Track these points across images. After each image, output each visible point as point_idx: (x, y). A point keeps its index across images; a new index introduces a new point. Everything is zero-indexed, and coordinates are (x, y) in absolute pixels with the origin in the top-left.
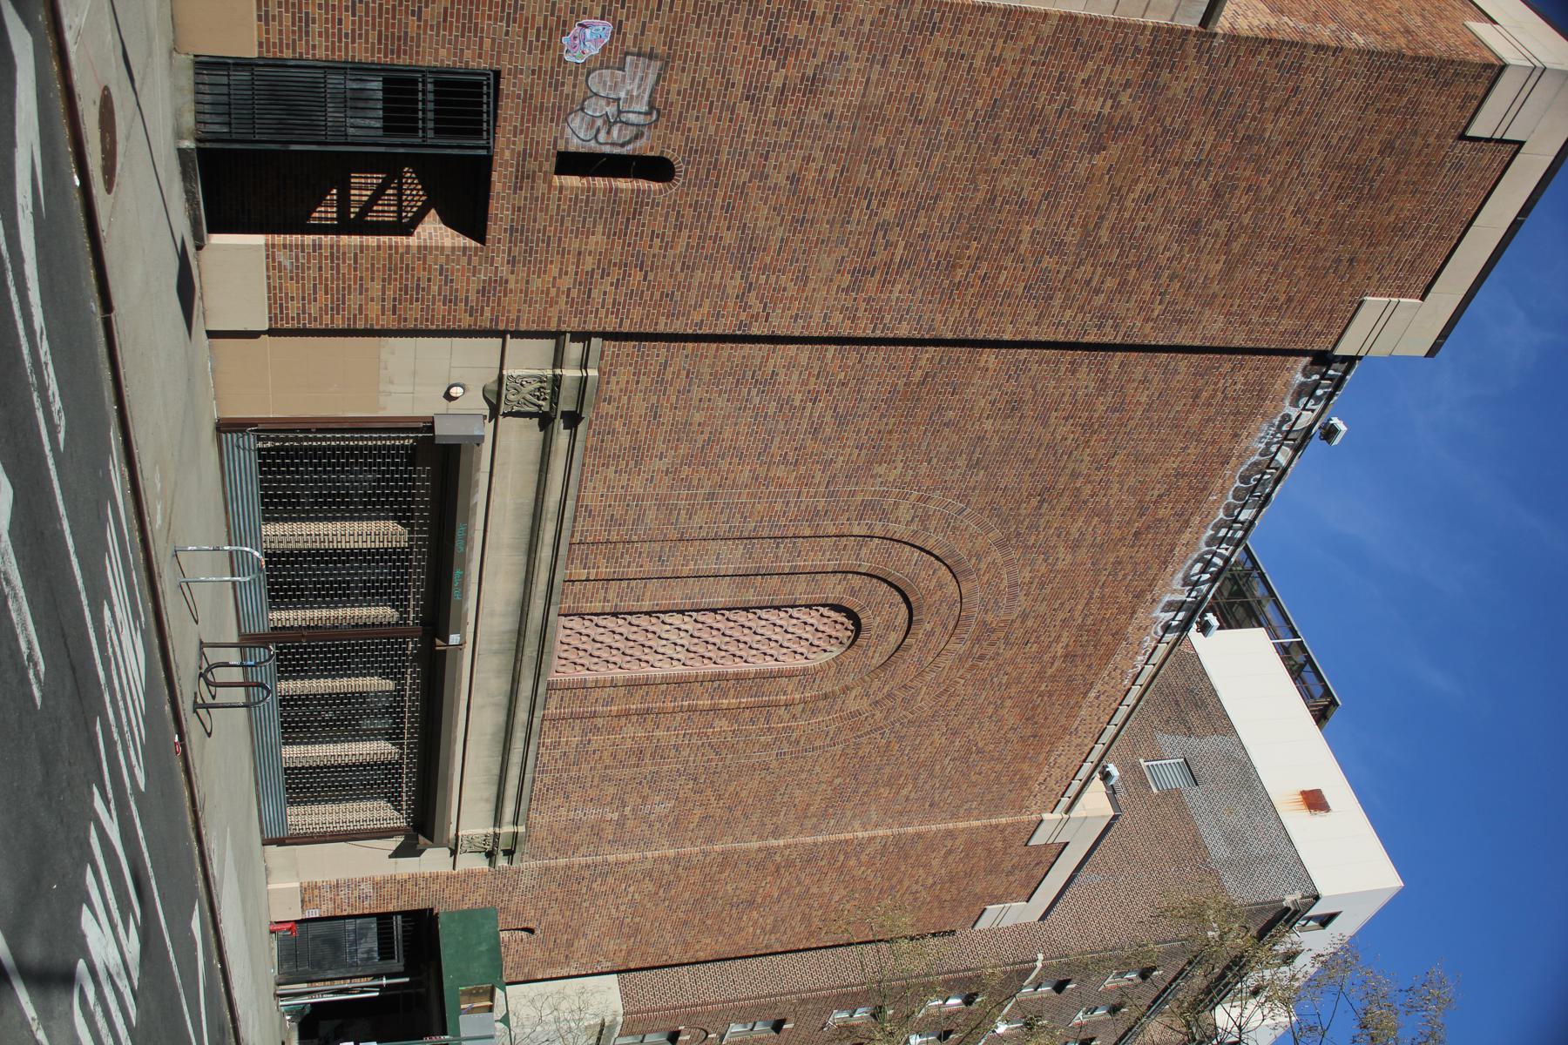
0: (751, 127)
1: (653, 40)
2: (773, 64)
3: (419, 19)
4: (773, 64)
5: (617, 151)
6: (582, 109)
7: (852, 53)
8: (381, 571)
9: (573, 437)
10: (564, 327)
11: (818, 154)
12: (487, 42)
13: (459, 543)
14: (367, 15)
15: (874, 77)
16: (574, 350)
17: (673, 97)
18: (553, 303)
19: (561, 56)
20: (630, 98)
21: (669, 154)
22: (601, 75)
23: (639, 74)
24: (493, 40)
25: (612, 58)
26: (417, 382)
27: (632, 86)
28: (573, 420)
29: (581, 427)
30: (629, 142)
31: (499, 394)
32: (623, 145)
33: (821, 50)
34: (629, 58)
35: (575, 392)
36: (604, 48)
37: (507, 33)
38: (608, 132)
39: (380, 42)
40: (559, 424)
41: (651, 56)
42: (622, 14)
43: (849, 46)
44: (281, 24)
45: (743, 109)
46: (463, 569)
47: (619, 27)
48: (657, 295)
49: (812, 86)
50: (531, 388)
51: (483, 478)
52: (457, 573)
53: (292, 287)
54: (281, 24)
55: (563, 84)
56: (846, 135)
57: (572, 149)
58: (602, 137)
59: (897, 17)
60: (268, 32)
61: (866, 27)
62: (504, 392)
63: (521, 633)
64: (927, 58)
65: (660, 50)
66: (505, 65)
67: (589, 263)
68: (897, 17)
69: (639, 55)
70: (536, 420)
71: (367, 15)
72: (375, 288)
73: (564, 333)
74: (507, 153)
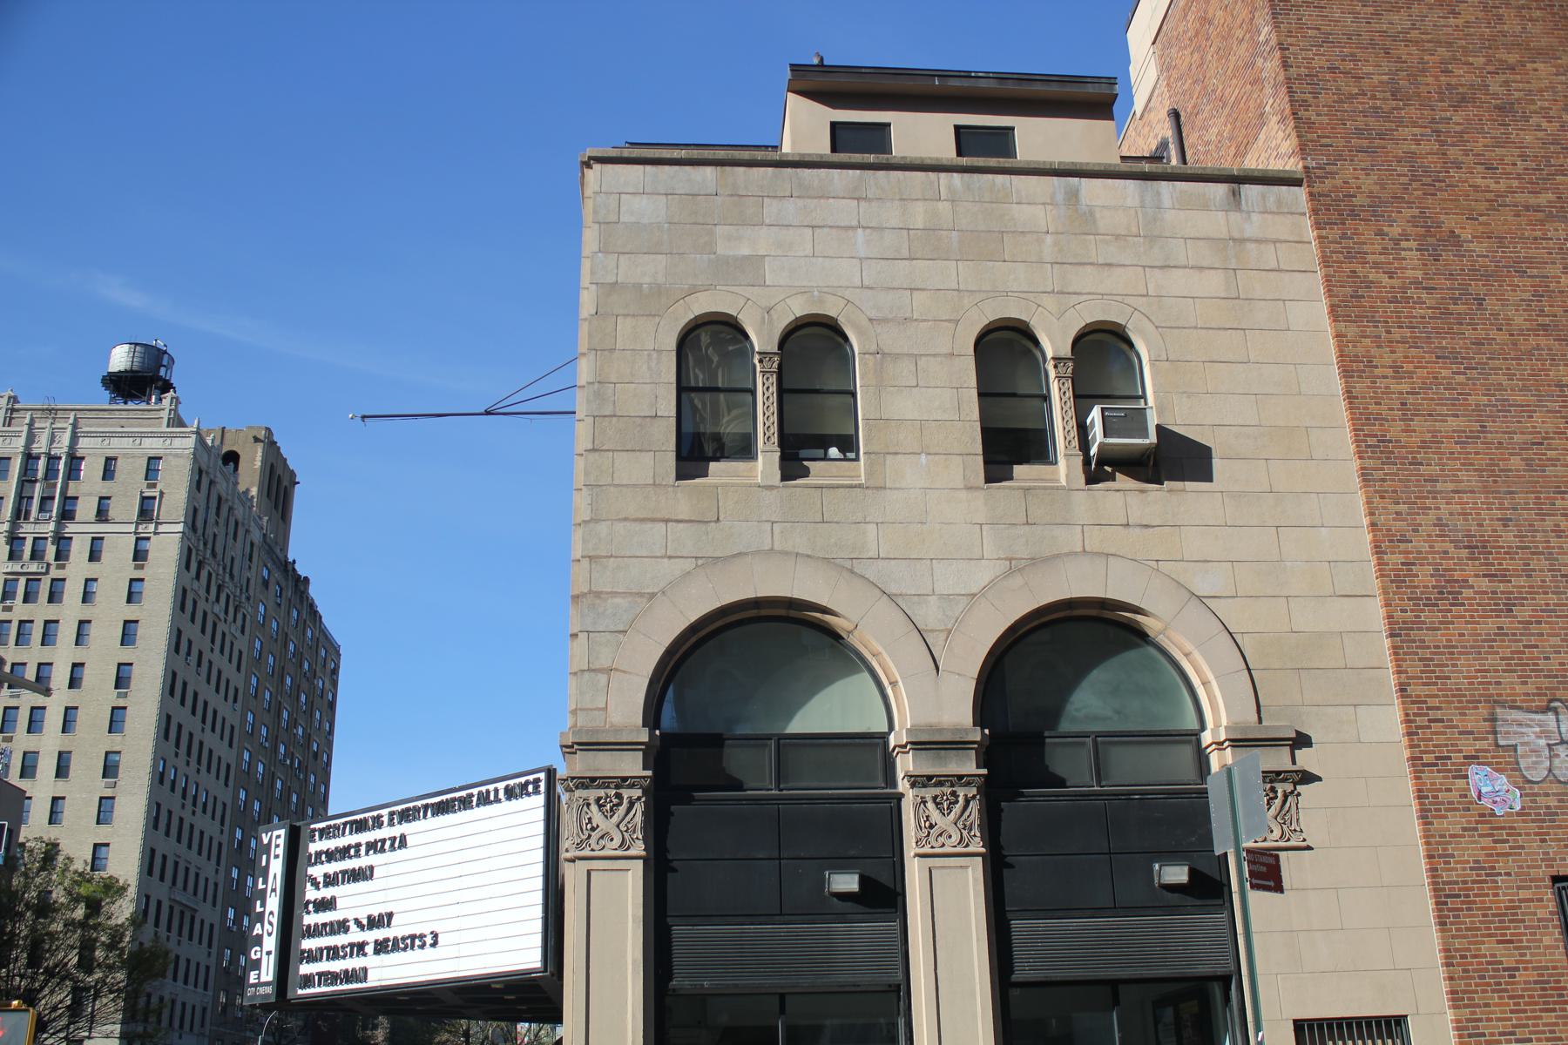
0: (1540, 600)
1: (1475, 719)
2: (1467, 593)
3: (1517, 969)
7: (1432, 515)
11: (1549, 523)
12: (1523, 894)
14: (1526, 1026)
15: (1450, 486)
17: (1531, 688)
19: (1518, 814)
20: (1545, 733)
22: (1528, 769)
23: (1515, 728)
24: (1519, 888)
25: (1505, 760)
27: (1531, 734)
33: (1438, 547)
34: (1501, 742)
36: (1496, 770)
37: (1508, 874)
39: (1554, 1010)
42: (1457, 758)
43: (1426, 521)
45: (1523, 613)
47: (1472, 758)
49: (1477, 548)
55: (1548, 807)
56: (1520, 499)
59: (1384, 480)
61: (1403, 508)
64: (1415, 439)
65: (1483, 711)
66: (1544, 872)
68: (1384, 480)
71: (1526, 1026)
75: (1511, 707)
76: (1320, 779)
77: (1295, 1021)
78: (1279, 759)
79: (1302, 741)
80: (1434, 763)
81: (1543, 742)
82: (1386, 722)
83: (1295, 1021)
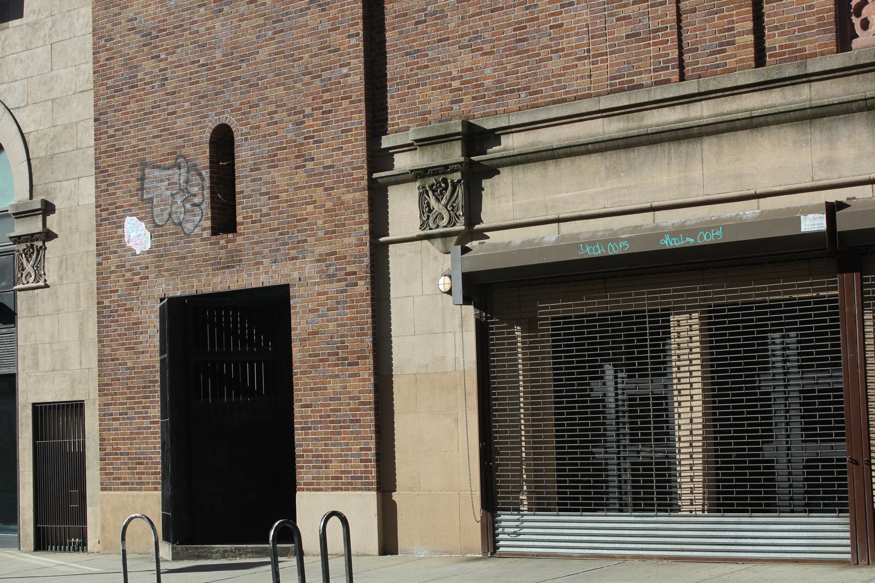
4: (140, 75)
5: (207, 183)
6: (180, 224)
8: (782, 346)
9: (508, 130)
10: (364, 183)
13: (614, 250)
16: (403, 162)
17: (166, 150)
18: (340, 203)
19: (148, 252)
21: (207, 136)
26: (435, 332)
28: (476, 138)
29: (489, 124)
30: (200, 175)
31: (444, 235)
32: (203, 179)
34: (145, 197)
35: (438, 147)
38: (195, 195)
40: (494, 152)
41: (142, 179)
44: (143, 473)
46: (662, 235)
48: (326, 96)
50: (433, 202)
51: (748, 210)
52: (668, 243)
53: (335, 467)
54: (143, 473)
57: (208, 224)
58: (197, 200)
60: (148, 483)
67: (300, 177)
69: (142, 189)
70: (486, 183)
72: (334, 386)
73: (371, 181)
74: (218, 279)
75: (154, 167)
76: (56, 236)
77: (34, 405)
78: (34, 226)
79: (48, 208)
80: (108, 218)
81: (169, 193)
82: (87, 189)
83: (34, 405)
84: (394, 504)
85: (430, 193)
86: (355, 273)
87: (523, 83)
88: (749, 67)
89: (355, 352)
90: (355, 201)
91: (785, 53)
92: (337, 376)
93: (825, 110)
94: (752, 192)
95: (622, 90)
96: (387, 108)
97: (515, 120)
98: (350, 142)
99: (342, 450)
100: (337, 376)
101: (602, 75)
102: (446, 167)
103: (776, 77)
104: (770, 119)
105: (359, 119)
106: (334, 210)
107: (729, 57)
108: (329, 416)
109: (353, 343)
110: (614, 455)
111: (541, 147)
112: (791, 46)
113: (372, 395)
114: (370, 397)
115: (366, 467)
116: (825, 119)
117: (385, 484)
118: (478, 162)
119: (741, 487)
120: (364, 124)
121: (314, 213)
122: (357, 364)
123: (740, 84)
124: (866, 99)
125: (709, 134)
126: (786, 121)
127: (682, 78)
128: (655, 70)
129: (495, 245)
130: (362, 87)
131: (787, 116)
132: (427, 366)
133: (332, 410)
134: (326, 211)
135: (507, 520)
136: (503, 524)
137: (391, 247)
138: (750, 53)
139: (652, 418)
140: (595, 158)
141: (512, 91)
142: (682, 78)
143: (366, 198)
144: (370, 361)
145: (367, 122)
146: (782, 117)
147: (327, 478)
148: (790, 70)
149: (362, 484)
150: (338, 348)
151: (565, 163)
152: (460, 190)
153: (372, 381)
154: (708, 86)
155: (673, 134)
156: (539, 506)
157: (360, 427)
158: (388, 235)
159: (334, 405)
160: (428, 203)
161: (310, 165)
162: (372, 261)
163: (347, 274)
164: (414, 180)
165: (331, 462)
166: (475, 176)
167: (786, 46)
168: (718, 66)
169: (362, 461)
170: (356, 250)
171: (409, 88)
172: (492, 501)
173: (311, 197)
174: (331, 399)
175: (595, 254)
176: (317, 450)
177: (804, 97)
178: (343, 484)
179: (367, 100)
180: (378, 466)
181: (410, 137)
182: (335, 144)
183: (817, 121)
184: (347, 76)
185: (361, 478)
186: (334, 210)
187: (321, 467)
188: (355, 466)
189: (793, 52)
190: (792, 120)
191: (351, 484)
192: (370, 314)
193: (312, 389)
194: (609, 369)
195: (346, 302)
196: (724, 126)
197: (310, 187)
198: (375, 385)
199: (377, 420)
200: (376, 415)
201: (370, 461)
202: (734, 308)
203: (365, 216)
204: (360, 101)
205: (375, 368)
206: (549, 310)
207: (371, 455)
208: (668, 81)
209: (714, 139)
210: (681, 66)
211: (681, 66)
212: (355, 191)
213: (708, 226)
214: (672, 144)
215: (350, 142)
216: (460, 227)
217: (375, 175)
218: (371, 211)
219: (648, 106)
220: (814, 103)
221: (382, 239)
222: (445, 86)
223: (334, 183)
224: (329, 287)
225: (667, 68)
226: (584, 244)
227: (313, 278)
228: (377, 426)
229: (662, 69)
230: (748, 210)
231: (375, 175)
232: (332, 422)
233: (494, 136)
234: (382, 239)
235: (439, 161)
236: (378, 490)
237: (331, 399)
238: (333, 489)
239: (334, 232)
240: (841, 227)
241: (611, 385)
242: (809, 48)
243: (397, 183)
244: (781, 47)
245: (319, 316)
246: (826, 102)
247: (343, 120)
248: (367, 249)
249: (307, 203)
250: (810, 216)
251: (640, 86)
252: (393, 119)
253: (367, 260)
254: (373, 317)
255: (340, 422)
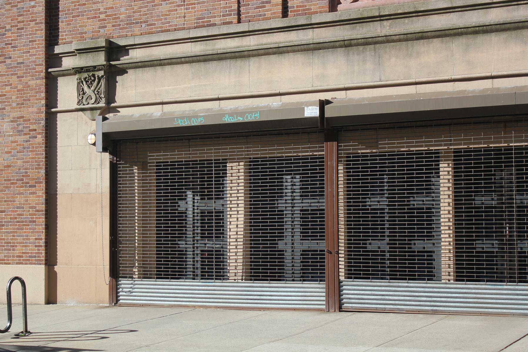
8: (291, 184)
9: (134, 46)
10: (43, 74)
13: (195, 122)
16: (68, 63)
28: (114, 51)
29: (122, 42)
31: (92, 109)
35: (90, 55)
40: (124, 60)
46: (224, 115)
48: (20, 19)
51: (275, 102)
52: (228, 120)
53: (19, 250)
62: (90, 106)
63: (347, 45)
70: (119, 78)
72: (20, 200)
84: (55, 273)
85: (84, 83)
86: (35, 130)
87: (144, 18)
88: (278, 17)
89: (33, 179)
90: (36, 85)
91: (299, 11)
92: (22, 194)
93: (321, 45)
94: (277, 92)
95: (204, 26)
96: (58, 29)
97: (138, 41)
98: (35, 48)
99: (24, 239)
100: (22, 194)
101: (191, 17)
102: (95, 67)
103: (293, 24)
104: (289, 49)
105: (41, 35)
106: (23, 90)
107: (267, 10)
108: (16, 218)
109: (32, 173)
110: (191, 245)
111: (153, 58)
112: (303, 6)
113: (44, 206)
114: (43, 207)
115: (38, 250)
116: (321, 51)
117: (50, 261)
118: (115, 65)
119: (265, 266)
120: (44, 38)
121: (10, 92)
122: (35, 186)
123: (273, 27)
124: (344, 41)
125: (254, 56)
126: (298, 51)
127: (239, 22)
128: (223, 16)
129: (123, 117)
130: (43, 14)
131: (299, 47)
132: (79, 189)
133: (18, 215)
134: (18, 91)
135: (125, 283)
136: (122, 286)
137: (59, 115)
138: (279, 9)
139: (213, 225)
140: (186, 67)
141: (137, 23)
142: (239, 22)
143: (44, 84)
144: (43, 185)
145: (46, 36)
146: (296, 48)
147: (13, 257)
148: (302, 21)
149: (36, 260)
150: (23, 176)
151: (168, 68)
152: (103, 82)
153: (44, 197)
154: (254, 27)
155: (233, 54)
156: (145, 275)
157: (36, 225)
158: (57, 107)
159: (19, 211)
160: (83, 89)
161: (8, 61)
162: (46, 123)
163: (30, 130)
164: (75, 74)
165: (16, 246)
166: (113, 73)
167: (300, 6)
168: (260, 16)
169: (36, 246)
170: (36, 116)
171: (73, 17)
172: (116, 272)
173: (9, 81)
174: (18, 208)
175: (184, 125)
176: (7, 239)
177: (309, 37)
178: (23, 260)
179: (46, 23)
180: (46, 250)
181: (73, 47)
182: (25, 49)
183: (316, 52)
184: (34, 7)
185: (35, 257)
186: (23, 90)
187: (10, 250)
188: (32, 249)
189: (304, 10)
190: (302, 51)
191: (29, 260)
192: (44, 156)
193: (5, 201)
194: (190, 194)
195: (29, 148)
196: (263, 51)
197: (8, 75)
198: (46, 200)
199: (46, 221)
200: (46, 218)
201: (41, 246)
202: (264, 159)
203: (43, 95)
204: (41, 23)
205: (46, 189)
206: (155, 157)
207: (42, 242)
208: (231, 23)
209: (256, 59)
210: (239, 14)
211: (239, 14)
212: (37, 79)
213: (251, 111)
214: (232, 60)
215: (35, 48)
216: (102, 104)
217: (50, 70)
218: (47, 92)
219: (219, 37)
220: (315, 41)
221: (53, 110)
222: (95, 17)
223: (24, 73)
224: (18, 138)
225: (231, 15)
226: (177, 118)
227: (9, 132)
228: (46, 225)
229: (228, 15)
230: (275, 102)
231: (50, 70)
232: (18, 222)
233: (124, 50)
234: (53, 110)
235: (91, 63)
236: (46, 264)
237: (18, 208)
238: (17, 264)
239: (23, 104)
240: (328, 114)
241: (190, 204)
242: (314, 8)
243: (64, 75)
244: (297, 7)
245: (12, 156)
246: (322, 41)
247: (30, 34)
248: (43, 115)
249: (6, 85)
250: (310, 107)
251: (214, 25)
252: (62, 36)
253: (43, 122)
254: (46, 157)
255: (23, 222)
